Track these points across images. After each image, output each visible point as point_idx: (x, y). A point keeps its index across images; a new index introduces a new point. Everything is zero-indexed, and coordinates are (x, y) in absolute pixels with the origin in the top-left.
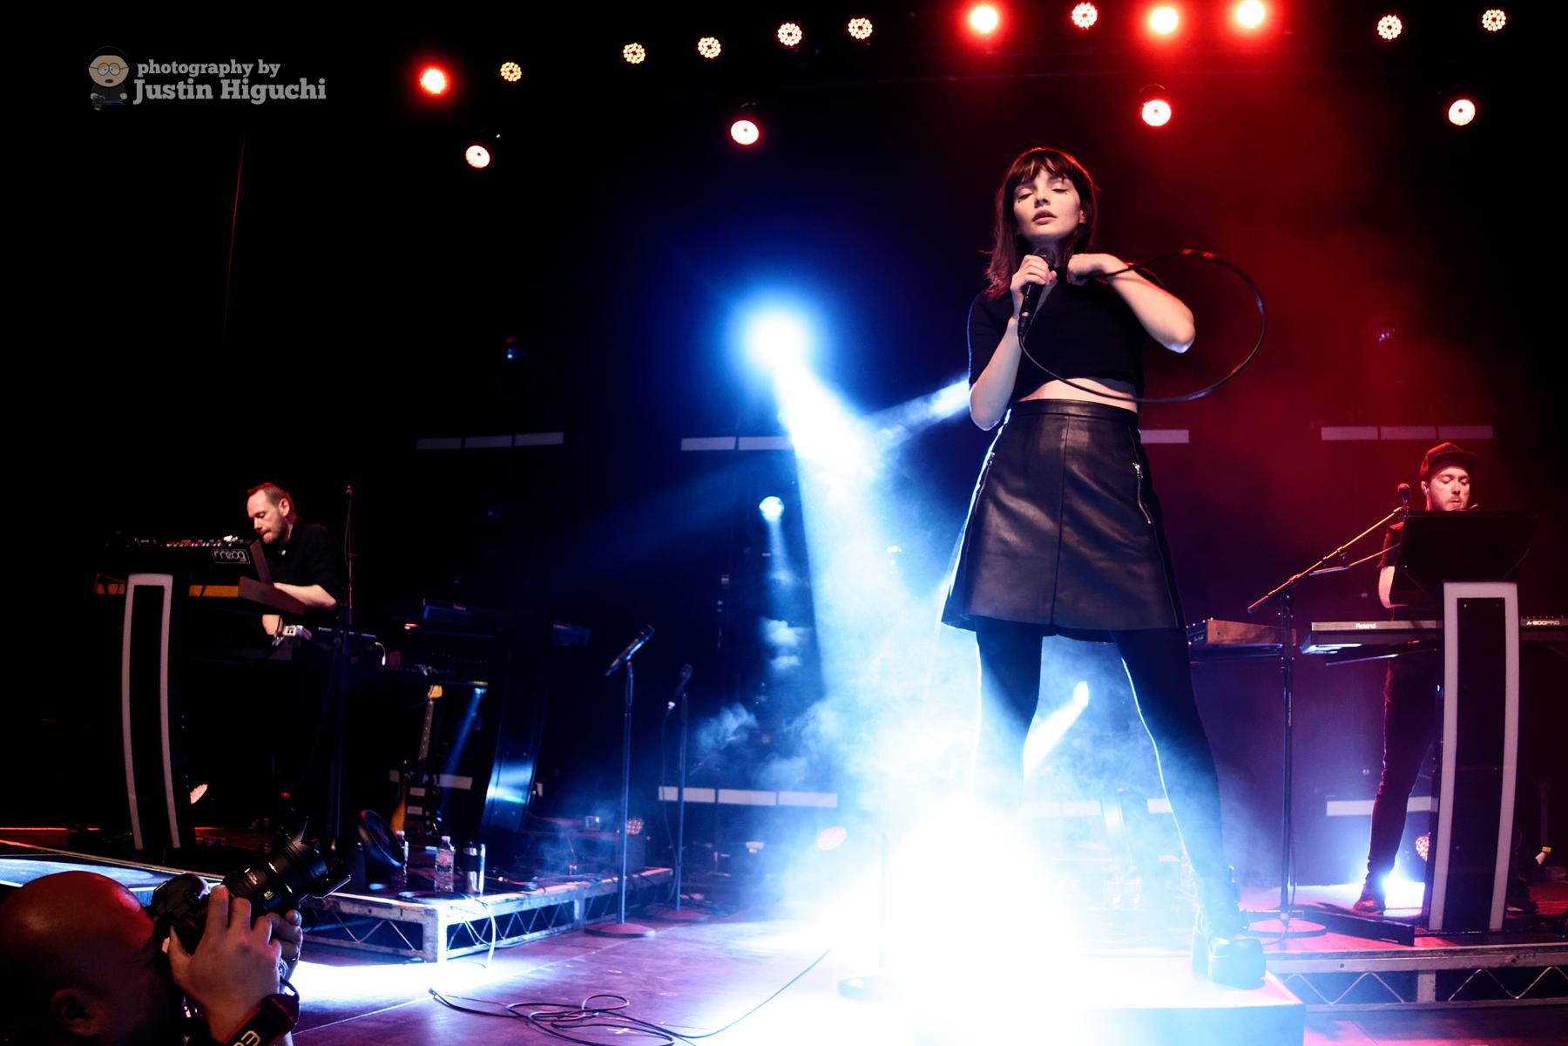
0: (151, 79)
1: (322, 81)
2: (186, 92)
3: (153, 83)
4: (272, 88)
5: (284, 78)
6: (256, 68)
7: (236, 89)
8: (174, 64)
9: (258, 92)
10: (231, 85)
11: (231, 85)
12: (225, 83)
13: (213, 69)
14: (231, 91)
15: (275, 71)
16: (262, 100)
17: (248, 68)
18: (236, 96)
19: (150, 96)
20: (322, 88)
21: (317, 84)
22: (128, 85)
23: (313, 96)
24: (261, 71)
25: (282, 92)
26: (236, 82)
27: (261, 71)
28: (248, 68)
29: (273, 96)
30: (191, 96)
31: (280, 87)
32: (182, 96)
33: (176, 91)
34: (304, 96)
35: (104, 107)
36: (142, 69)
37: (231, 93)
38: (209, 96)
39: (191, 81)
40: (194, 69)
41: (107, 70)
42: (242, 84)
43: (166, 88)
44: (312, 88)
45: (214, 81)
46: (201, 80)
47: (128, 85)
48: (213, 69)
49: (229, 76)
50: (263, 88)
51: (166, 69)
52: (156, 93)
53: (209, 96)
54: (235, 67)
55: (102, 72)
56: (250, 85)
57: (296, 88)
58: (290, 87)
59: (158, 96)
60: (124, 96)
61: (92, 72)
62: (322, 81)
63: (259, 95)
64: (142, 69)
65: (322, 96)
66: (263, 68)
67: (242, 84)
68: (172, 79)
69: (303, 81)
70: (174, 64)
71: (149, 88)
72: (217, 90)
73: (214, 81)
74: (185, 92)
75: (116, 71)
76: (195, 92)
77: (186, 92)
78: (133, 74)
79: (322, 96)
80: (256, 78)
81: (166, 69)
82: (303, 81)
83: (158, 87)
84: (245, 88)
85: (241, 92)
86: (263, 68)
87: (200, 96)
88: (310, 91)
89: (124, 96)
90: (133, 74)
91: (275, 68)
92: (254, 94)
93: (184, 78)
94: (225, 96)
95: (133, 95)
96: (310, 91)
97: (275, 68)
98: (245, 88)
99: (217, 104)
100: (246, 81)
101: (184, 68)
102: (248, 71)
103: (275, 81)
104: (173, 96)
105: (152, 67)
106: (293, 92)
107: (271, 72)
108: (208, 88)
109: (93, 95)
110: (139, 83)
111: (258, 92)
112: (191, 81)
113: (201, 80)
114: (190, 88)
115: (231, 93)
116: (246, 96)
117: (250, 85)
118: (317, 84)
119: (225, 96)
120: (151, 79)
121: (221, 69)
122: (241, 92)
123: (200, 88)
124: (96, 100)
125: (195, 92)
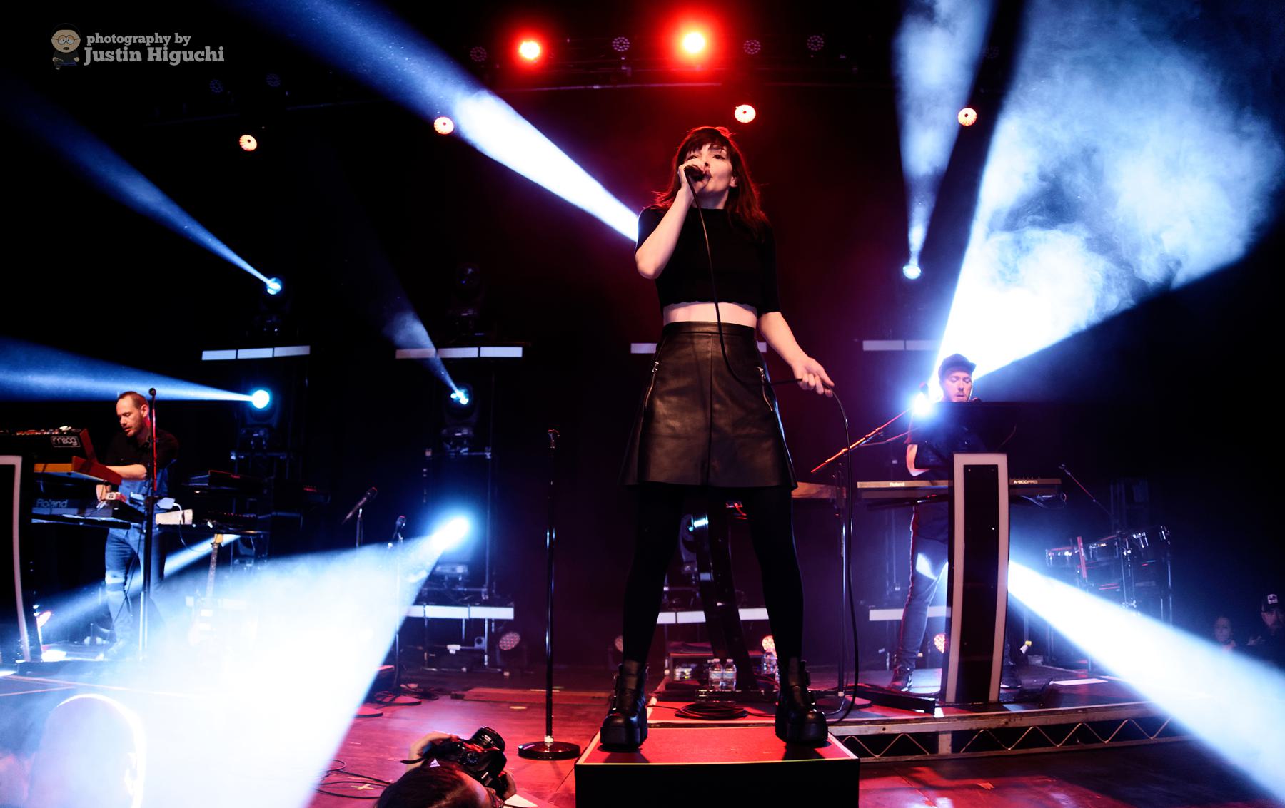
0: (96, 47)
2: (122, 56)
4: (185, 53)
5: (193, 47)
6: (173, 39)
7: (158, 54)
12: (150, 50)
13: (142, 39)
14: (155, 55)
17: (167, 39)
18: (158, 59)
19: (96, 59)
20: (221, 54)
21: (217, 51)
22: (80, 52)
23: (215, 59)
26: (159, 49)
28: (167, 39)
29: (186, 59)
30: (126, 59)
31: (191, 53)
32: (119, 60)
34: (208, 59)
35: (63, 68)
38: (139, 59)
40: (129, 40)
41: (65, 40)
42: (162, 50)
43: (107, 53)
44: (214, 53)
45: (143, 49)
46: (133, 47)
47: (80, 52)
48: (142, 39)
49: (153, 45)
50: (178, 53)
52: (100, 57)
53: (139, 59)
54: (158, 38)
56: (169, 52)
58: (198, 53)
59: (102, 59)
60: (77, 59)
61: (54, 42)
63: (175, 59)
64: (90, 40)
65: (221, 59)
66: (179, 39)
67: (162, 50)
68: (112, 47)
69: (208, 48)
71: (95, 53)
72: (145, 55)
73: (143, 49)
74: (122, 56)
75: (71, 41)
77: (122, 56)
78: (83, 43)
79: (221, 59)
80: (173, 47)
82: (208, 48)
83: (101, 53)
84: (165, 54)
86: (179, 39)
87: (132, 59)
88: (212, 55)
89: (77, 59)
90: (83, 43)
91: (187, 39)
92: (172, 58)
93: (121, 46)
94: (150, 59)
95: (83, 59)
96: (212, 55)
97: (187, 39)
98: (165, 54)
99: (147, 69)
101: (121, 39)
103: (187, 49)
104: (112, 59)
105: (98, 38)
108: (138, 53)
110: (88, 50)
113: (133, 47)
114: (125, 54)
116: (166, 59)
117: (169, 52)
118: (217, 51)
119: (150, 59)
120: (96, 47)
121: (149, 40)
123: (132, 53)
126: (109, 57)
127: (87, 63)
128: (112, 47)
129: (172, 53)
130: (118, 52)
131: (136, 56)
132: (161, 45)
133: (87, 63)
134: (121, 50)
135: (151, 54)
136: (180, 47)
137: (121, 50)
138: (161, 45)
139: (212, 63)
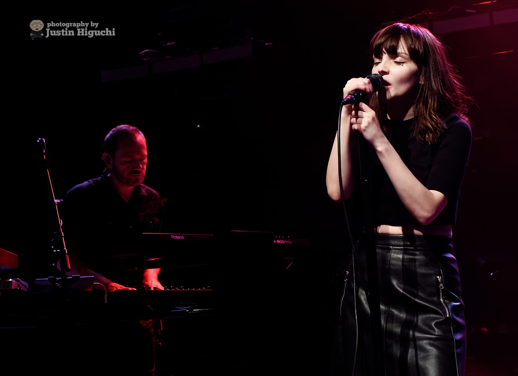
0: (52, 28)
1: (114, 29)
2: (65, 33)
3: (53, 30)
4: (96, 31)
5: (100, 28)
6: (90, 24)
8: (60, 23)
9: (91, 33)
10: (81, 31)
11: (81, 31)
12: (79, 30)
13: (74, 25)
14: (81, 33)
15: (97, 26)
17: (87, 24)
18: (83, 35)
19: (52, 35)
20: (114, 32)
21: (112, 30)
22: (44, 31)
23: (111, 35)
24: (92, 26)
25: (99, 33)
26: (83, 30)
27: (92, 26)
29: (96, 35)
30: (66, 34)
31: (99, 31)
32: (63, 35)
33: (61, 33)
34: (107, 35)
35: (35, 39)
36: (49, 25)
37: (81, 33)
38: (73, 34)
39: (66, 29)
40: (68, 25)
41: (36, 25)
42: (85, 30)
43: (57, 31)
44: (110, 31)
45: (75, 29)
46: (70, 29)
47: (44, 31)
48: (74, 25)
49: (80, 27)
50: (92, 32)
51: (57, 25)
52: (54, 33)
53: (73, 34)
54: (82, 24)
55: (34, 26)
56: (88, 31)
57: (104, 32)
58: (102, 31)
59: (55, 34)
61: (31, 26)
63: (91, 34)
64: (49, 25)
65: (114, 34)
66: (92, 24)
67: (85, 30)
68: (60, 28)
69: (107, 29)
70: (60, 23)
71: (51, 32)
72: (76, 32)
73: (75, 29)
75: (39, 26)
76: (68, 33)
77: (65, 33)
78: (46, 26)
79: (114, 34)
80: (90, 28)
81: (57, 25)
82: (107, 29)
83: (54, 31)
84: (86, 32)
85: (84, 33)
86: (92, 24)
87: (70, 35)
88: (109, 33)
89: (42, 35)
90: (46, 26)
91: (97, 25)
92: (89, 34)
93: (64, 28)
94: (79, 34)
95: (45, 34)
96: (109, 33)
97: (97, 25)
98: (86, 32)
100: (86, 29)
101: (64, 25)
102: (87, 26)
103: (97, 29)
104: (60, 34)
105: (53, 24)
106: (103, 33)
107: (95, 26)
108: (73, 32)
109: (31, 34)
110: (48, 30)
111: (91, 33)
112: (66, 29)
113: (70, 29)
114: (66, 32)
115: (81, 33)
116: (86, 35)
117: (88, 31)
119: (79, 34)
120: (52, 28)
121: (78, 25)
122: (84, 33)
123: (70, 32)
124: (32, 36)
125: (68, 33)
126: (58, 33)
127: (47, 36)
128: (60, 28)
129: (89, 31)
130: (63, 31)
131: (72, 33)
132: (84, 28)
133: (47, 36)
134: (64, 30)
135: (79, 32)
136: (93, 29)
137: (64, 30)
138: (84, 28)
139: (109, 36)
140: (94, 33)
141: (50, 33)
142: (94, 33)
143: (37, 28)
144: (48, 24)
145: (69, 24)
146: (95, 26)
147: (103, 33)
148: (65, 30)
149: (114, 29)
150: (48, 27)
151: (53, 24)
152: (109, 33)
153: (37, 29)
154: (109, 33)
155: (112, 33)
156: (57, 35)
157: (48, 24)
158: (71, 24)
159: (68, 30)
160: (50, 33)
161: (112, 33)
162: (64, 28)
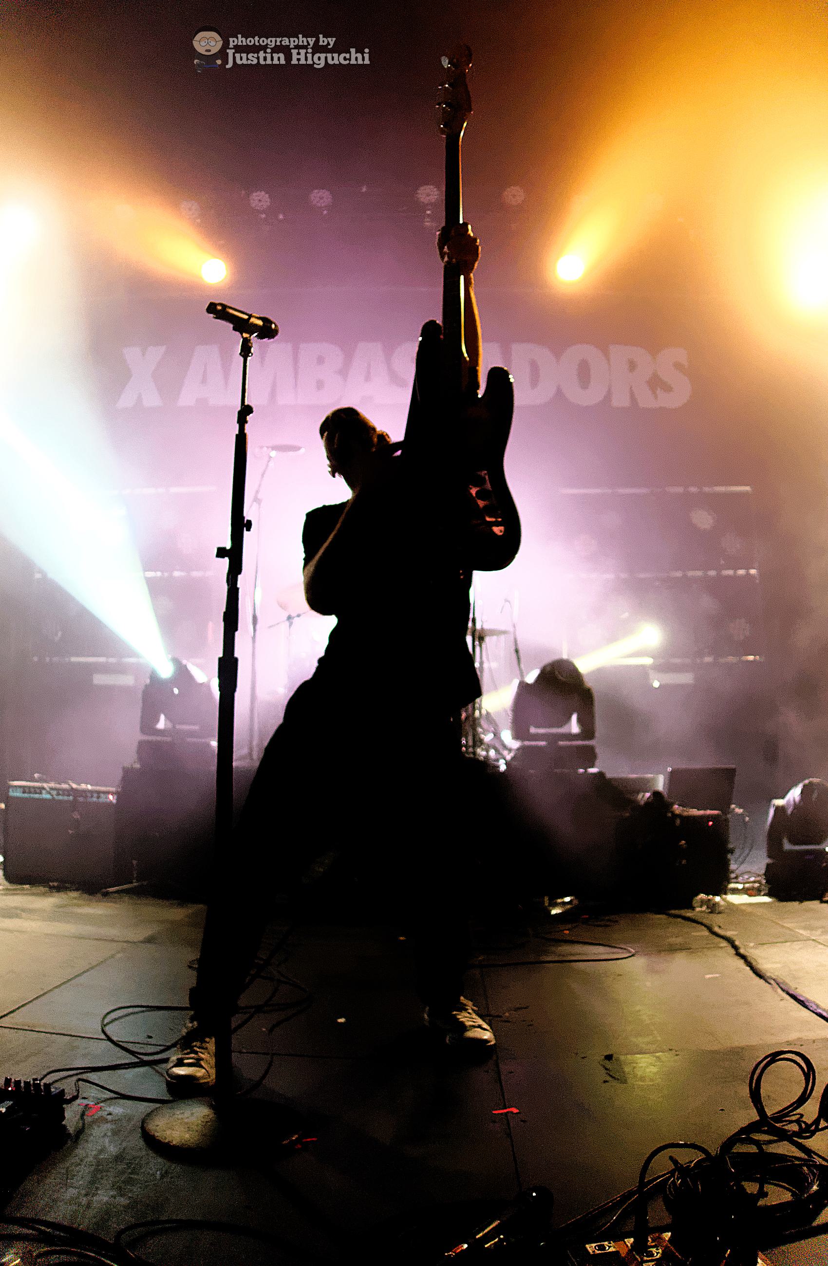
0: (238, 49)
2: (265, 59)
4: (329, 56)
5: (338, 49)
6: (318, 40)
7: (302, 57)
8: (257, 38)
9: (319, 59)
10: (299, 54)
11: (299, 54)
12: (294, 52)
13: (286, 41)
14: (299, 58)
15: (332, 43)
16: (322, 65)
17: (312, 41)
18: (303, 62)
19: (239, 62)
20: (367, 56)
21: (363, 53)
22: (222, 54)
23: (360, 62)
24: (321, 43)
26: (303, 52)
27: (321, 43)
28: (312, 41)
29: (330, 62)
30: (269, 62)
31: (336, 55)
32: (262, 62)
33: (258, 58)
34: (353, 62)
36: (233, 41)
37: (299, 60)
39: (269, 50)
40: (272, 42)
41: (207, 42)
43: (250, 56)
44: (359, 56)
45: (286, 51)
46: (277, 49)
48: (286, 41)
49: (297, 47)
50: (323, 56)
51: (250, 42)
52: (243, 59)
53: (283, 62)
54: (302, 40)
55: (203, 43)
56: (313, 54)
57: (348, 56)
58: (343, 55)
59: (244, 62)
61: (195, 44)
62: (367, 50)
63: (320, 61)
64: (233, 41)
66: (323, 41)
68: (256, 49)
69: (353, 50)
70: (257, 38)
71: (238, 56)
72: (289, 57)
73: (286, 51)
74: (265, 58)
75: (213, 43)
76: (272, 59)
77: (265, 59)
78: (226, 45)
79: (367, 62)
80: (318, 49)
81: (250, 42)
82: (353, 50)
83: (244, 55)
84: (309, 56)
85: (306, 59)
86: (323, 41)
87: (276, 62)
88: (358, 58)
89: (219, 62)
90: (226, 45)
91: (332, 41)
93: (264, 48)
96: (358, 58)
97: (332, 41)
98: (309, 56)
100: (310, 51)
101: (264, 41)
102: (312, 43)
103: (332, 51)
104: (255, 62)
105: (241, 40)
106: (345, 59)
107: (329, 44)
108: (282, 56)
109: (196, 61)
110: (230, 52)
111: (319, 59)
112: (269, 50)
113: (277, 49)
114: (269, 56)
115: (299, 60)
116: (310, 62)
117: (313, 54)
118: (363, 53)
119: (294, 62)
120: (238, 49)
121: (292, 42)
122: (306, 59)
123: (275, 56)
125: (272, 59)
126: (252, 59)
127: (230, 65)
129: (316, 56)
131: (279, 59)
132: (305, 47)
133: (230, 65)
136: (324, 49)
138: (305, 47)
140: (326, 58)
141: (234, 58)
142: (326, 58)
143: (208, 48)
144: (231, 40)
145: (273, 39)
146: (329, 44)
147: (345, 59)
148: (265, 52)
149: (367, 50)
150: (231, 46)
151: (241, 40)
152: (356, 59)
153: (210, 51)
154: (356, 59)
155: (363, 59)
156: (249, 62)
157: (231, 40)
158: (279, 40)
159: (272, 53)
160: (234, 58)
161: (363, 59)
162: (264, 48)
